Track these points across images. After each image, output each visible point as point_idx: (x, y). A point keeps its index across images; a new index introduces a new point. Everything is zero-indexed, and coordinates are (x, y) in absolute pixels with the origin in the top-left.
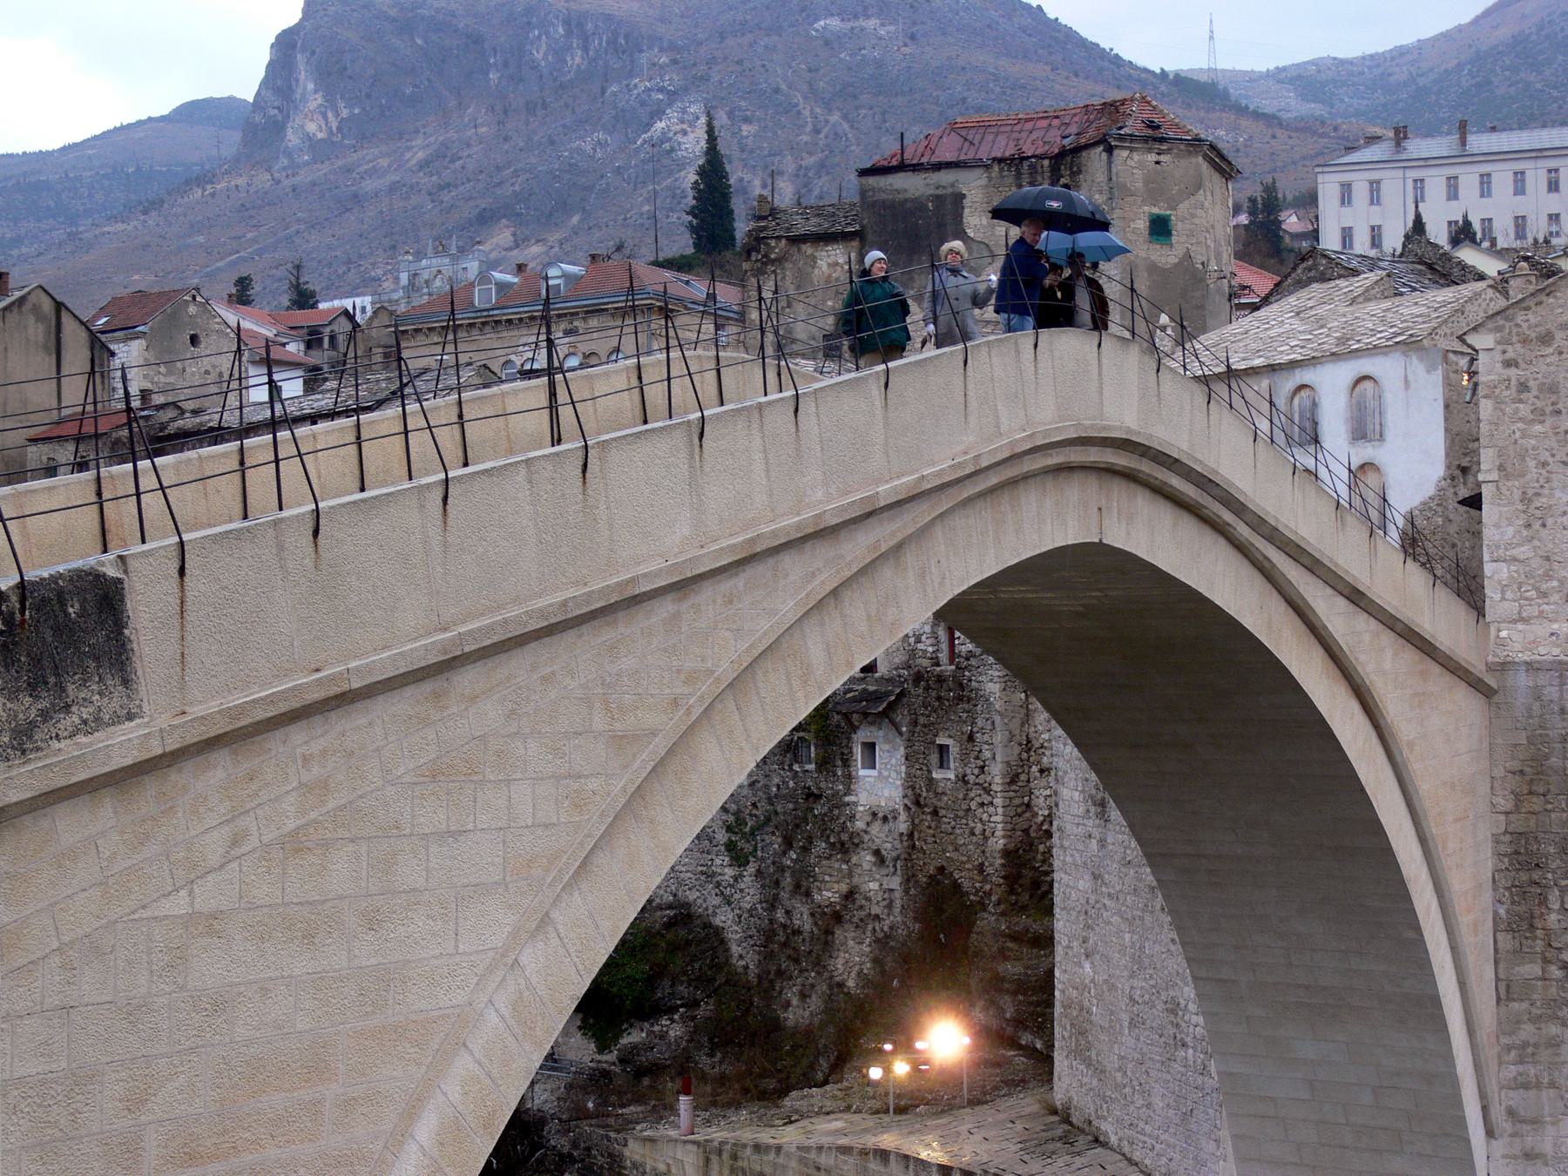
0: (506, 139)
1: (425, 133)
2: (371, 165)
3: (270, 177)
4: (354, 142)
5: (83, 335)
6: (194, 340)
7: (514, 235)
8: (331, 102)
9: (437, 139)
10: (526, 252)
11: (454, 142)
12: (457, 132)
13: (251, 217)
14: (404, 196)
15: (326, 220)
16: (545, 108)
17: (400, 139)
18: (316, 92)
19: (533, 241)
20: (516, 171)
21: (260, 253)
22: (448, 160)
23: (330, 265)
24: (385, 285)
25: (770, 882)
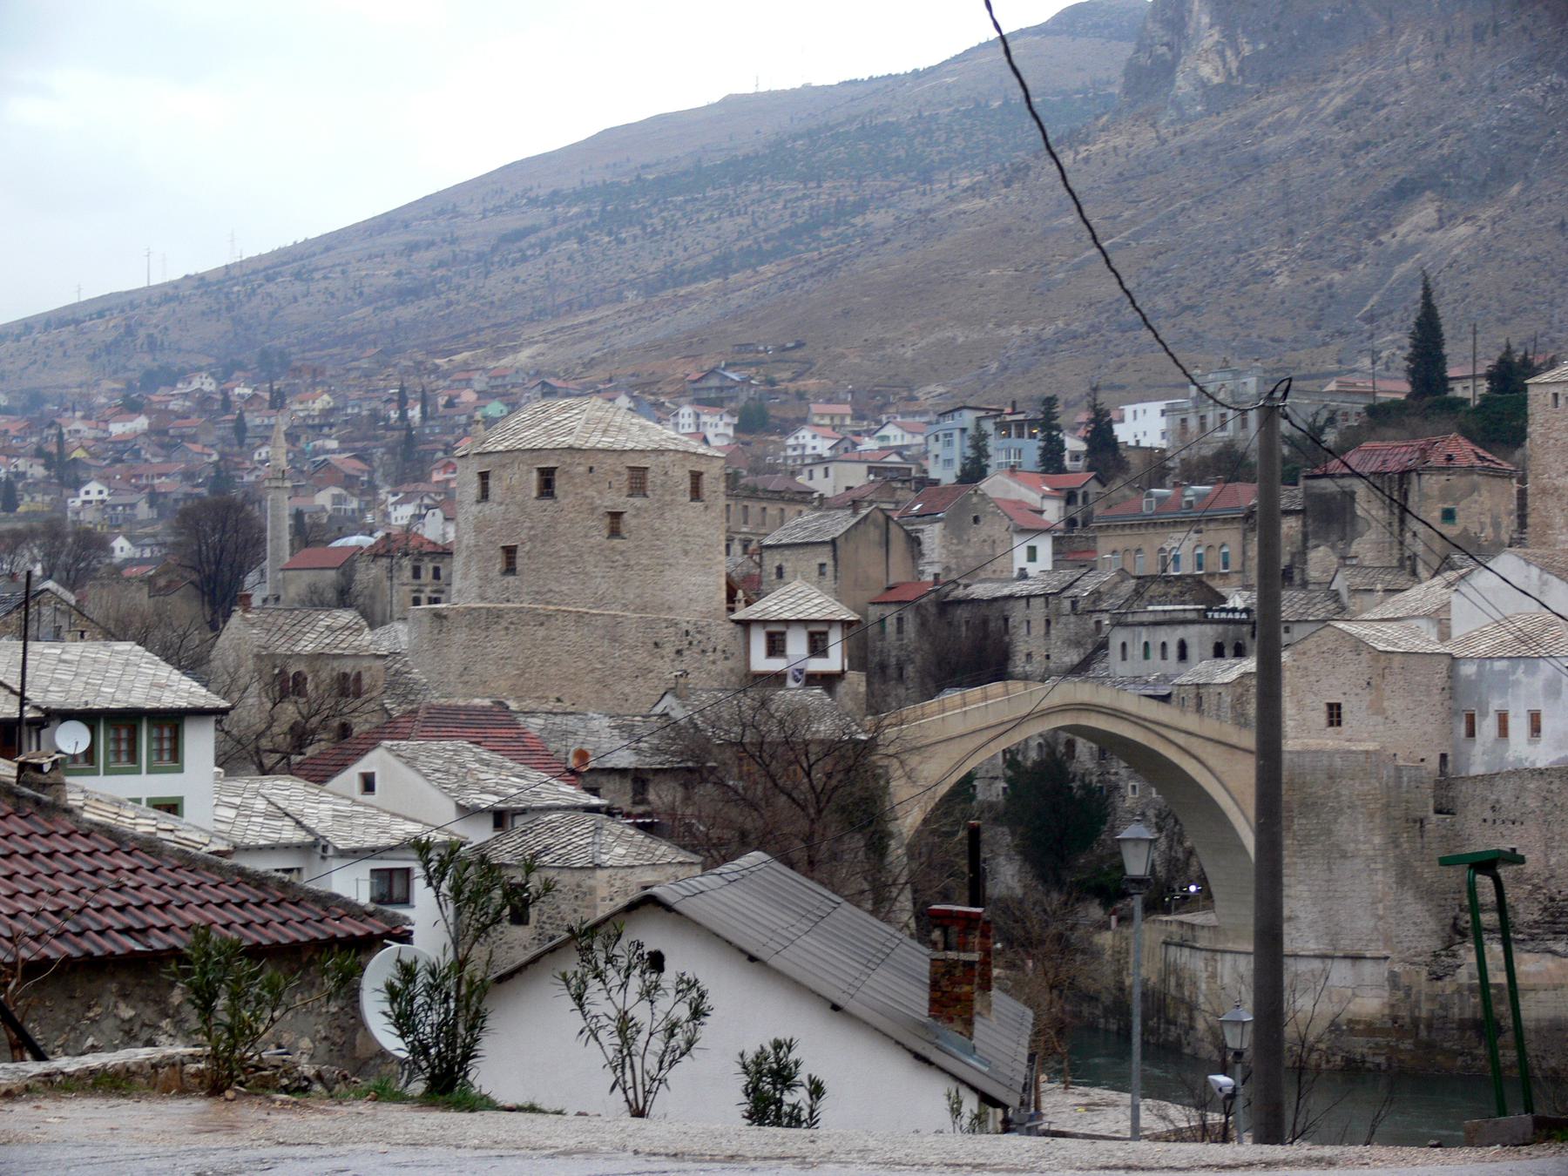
0: (1445, 78)
1: (1345, 72)
2: (1276, 116)
3: (1154, 135)
4: (1257, 85)
5: (902, 534)
6: (976, 520)
7: (1439, 211)
8: (1230, 39)
9: (1359, 80)
10: (1451, 234)
11: (1380, 82)
12: (1384, 68)
13: (1130, 190)
14: (1312, 158)
15: (1218, 192)
16: (1496, 34)
17: (1315, 80)
18: (1211, 26)
19: (1461, 219)
20: (1444, 129)
21: (1136, 236)
22: (1370, 107)
23: (1216, 254)
24: (1279, 279)
25: (1170, 839)
